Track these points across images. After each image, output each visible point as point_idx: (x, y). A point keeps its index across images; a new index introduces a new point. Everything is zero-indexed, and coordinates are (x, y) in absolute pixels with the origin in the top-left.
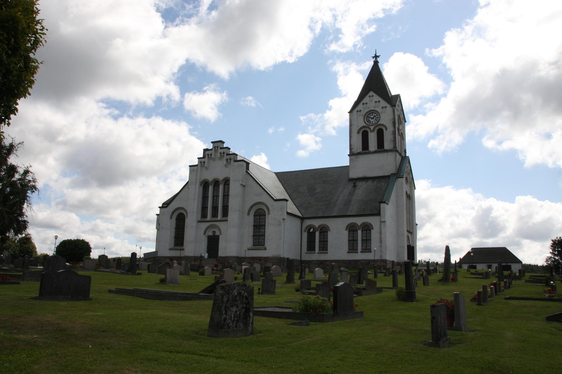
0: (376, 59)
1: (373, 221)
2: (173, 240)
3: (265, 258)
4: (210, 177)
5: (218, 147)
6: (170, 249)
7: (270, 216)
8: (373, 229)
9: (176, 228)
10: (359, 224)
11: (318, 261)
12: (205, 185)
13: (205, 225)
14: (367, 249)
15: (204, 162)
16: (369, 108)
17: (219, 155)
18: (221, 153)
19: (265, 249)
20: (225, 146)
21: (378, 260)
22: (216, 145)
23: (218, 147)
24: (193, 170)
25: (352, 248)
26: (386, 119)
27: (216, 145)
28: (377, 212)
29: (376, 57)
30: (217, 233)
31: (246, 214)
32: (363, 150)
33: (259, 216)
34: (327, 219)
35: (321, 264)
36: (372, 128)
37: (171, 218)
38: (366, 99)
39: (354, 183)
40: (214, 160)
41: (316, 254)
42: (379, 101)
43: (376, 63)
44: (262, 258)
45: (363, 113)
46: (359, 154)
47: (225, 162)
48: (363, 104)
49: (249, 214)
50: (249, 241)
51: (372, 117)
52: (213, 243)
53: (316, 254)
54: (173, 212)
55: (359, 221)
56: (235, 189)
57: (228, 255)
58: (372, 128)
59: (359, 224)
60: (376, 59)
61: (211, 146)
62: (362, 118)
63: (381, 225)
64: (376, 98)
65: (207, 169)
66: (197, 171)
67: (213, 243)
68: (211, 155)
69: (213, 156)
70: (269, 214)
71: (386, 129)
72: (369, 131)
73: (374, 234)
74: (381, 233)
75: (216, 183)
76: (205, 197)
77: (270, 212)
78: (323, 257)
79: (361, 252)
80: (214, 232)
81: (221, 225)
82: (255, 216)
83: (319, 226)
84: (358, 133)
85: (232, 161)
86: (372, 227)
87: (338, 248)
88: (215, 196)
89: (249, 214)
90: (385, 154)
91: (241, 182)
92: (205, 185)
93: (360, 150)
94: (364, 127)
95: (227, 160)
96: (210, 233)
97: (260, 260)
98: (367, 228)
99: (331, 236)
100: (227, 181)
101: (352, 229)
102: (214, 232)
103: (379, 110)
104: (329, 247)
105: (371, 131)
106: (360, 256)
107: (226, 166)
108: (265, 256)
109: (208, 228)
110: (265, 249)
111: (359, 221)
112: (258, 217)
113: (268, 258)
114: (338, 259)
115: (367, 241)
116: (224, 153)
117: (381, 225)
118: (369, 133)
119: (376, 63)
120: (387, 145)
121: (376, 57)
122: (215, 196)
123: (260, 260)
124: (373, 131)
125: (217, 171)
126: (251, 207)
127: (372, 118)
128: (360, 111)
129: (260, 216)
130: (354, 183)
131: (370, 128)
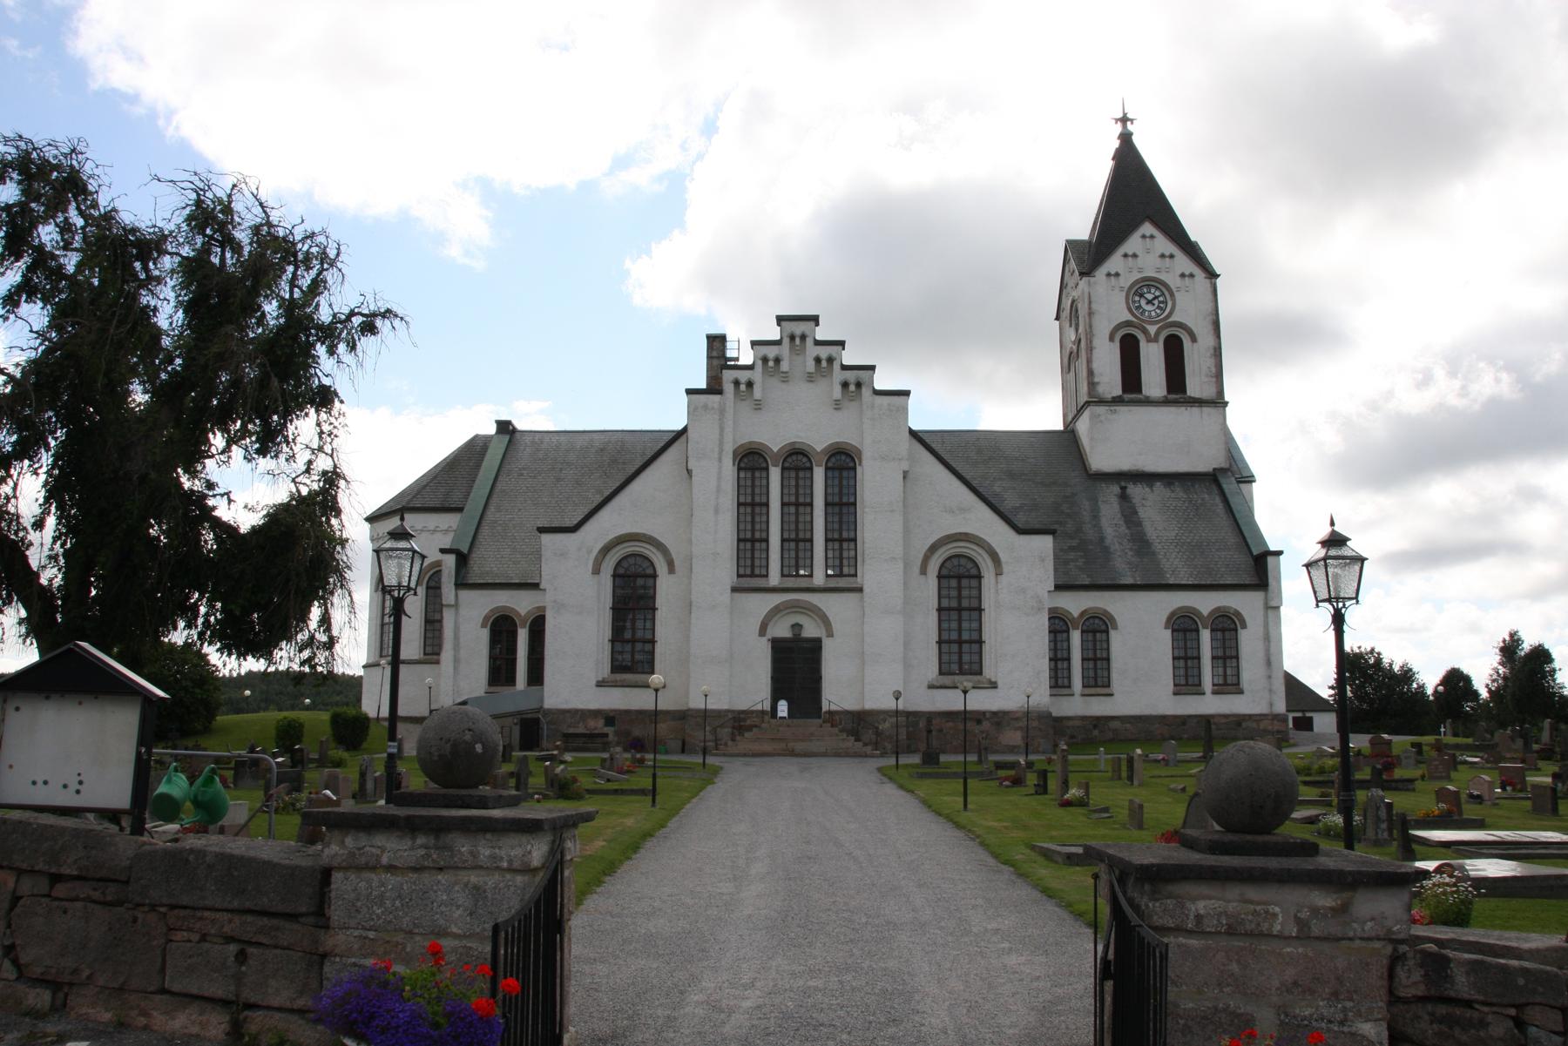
0: (1125, 126)
1: (1244, 603)
2: (608, 647)
3: (995, 714)
4: (774, 434)
5: (803, 337)
6: (600, 684)
7: (1003, 579)
8: (1244, 626)
9: (613, 609)
10: (1205, 612)
11: (1084, 718)
12: (751, 460)
13: (761, 604)
14: (1229, 684)
15: (750, 384)
16: (1140, 270)
17: (810, 366)
18: (818, 360)
19: (993, 685)
20: (821, 333)
21: (1262, 717)
22: (798, 328)
23: (803, 337)
24: (705, 407)
25: (1187, 682)
26: (1187, 310)
27: (798, 328)
28: (1255, 581)
29: (1124, 120)
30: (811, 630)
31: (917, 569)
32: (1124, 391)
33: (959, 581)
34: (1107, 595)
35: (1095, 727)
36: (1152, 329)
37: (596, 571)
38: (1133, 244)
39: (1123, 489)
40: (785, 378)
41: (1077, 697)
42: (1172, 256)
43: (1126, 138)
44: (984, 713)
45: (1127, 280)
46: (1117, 401)
47: (837, 392)
48: (1126, 256)
49: (923, 571)
50: (928, 663)
51: (1150, 297)
52: (796, 666)
53: (1077, 697)
54: (606, 550)
55: (1205, 603)
56: (876, 485)
57: (870, 704)
58: (1152, 329)
59: (1205, 612)
60: (1125, 126)
61: (774, 333)
62: (1120, 299)
63: (1266, 617)
64: (1163, 244)
65: (758, 406)
66: (722, 411)
67: (796, 666)
68: (777, 360)
69: (785, 366)
70: (999, 573)
71: (1194, 339)
72: (1141, 337)
73: (1249, 642)
74: (1267, 638)
75: (797, 460)
76: (751, 506)
77: (1005, 568)
78: (1099, 707)
79: (1214, 693)
80: (797, 627)
81: (831, 604)
82: (940, 577)
83: (1082, 614)
84: (1111, 339)
85: (866, 392)
86: (1112, 619)
87: (1143, 681)
88: (797, 505)
89: (923, 571)
90: (1195, 410)
91: (905, 466)
92: (751, 460)
93: (1117, 391)
94: (1128, 324)
95: (845, 385)
96: (782, 630)
97: (979, 722)
98: (1227, 625)
99: (1119, 644)
100: (843, 461)
101: (1183, 626)
102: (797, 627)
103: (1172, 280)
104: (1114, 676)
105: (1149, 340)
106: (1209, 704)
107: (837, 406)
108: (994, 708)
109: (776, 611)
110: (993, 685)
111: (1205, 603)
112: (954, 583)
113: (1005, 713)
114: (1147, 712)
115: (1228, 656)
116: (830, 360)
117: (1266, 617)
118: (1143, 345)
119: (1126, 138)
120: (1194, 388)
121: (1124, 120)
122: (797, 505)
123: (979, 722)
124: (1155, 340)
125: (800, 418)
126: (933, 549)
127: (1149, 302)
128: (1117, 275)
129: (959, 577)
130: (1123, 489)
131: (1145, 331)
